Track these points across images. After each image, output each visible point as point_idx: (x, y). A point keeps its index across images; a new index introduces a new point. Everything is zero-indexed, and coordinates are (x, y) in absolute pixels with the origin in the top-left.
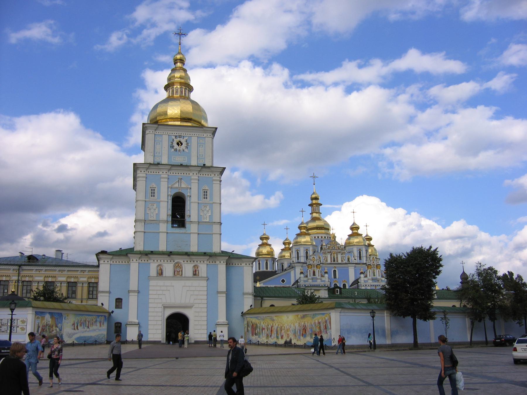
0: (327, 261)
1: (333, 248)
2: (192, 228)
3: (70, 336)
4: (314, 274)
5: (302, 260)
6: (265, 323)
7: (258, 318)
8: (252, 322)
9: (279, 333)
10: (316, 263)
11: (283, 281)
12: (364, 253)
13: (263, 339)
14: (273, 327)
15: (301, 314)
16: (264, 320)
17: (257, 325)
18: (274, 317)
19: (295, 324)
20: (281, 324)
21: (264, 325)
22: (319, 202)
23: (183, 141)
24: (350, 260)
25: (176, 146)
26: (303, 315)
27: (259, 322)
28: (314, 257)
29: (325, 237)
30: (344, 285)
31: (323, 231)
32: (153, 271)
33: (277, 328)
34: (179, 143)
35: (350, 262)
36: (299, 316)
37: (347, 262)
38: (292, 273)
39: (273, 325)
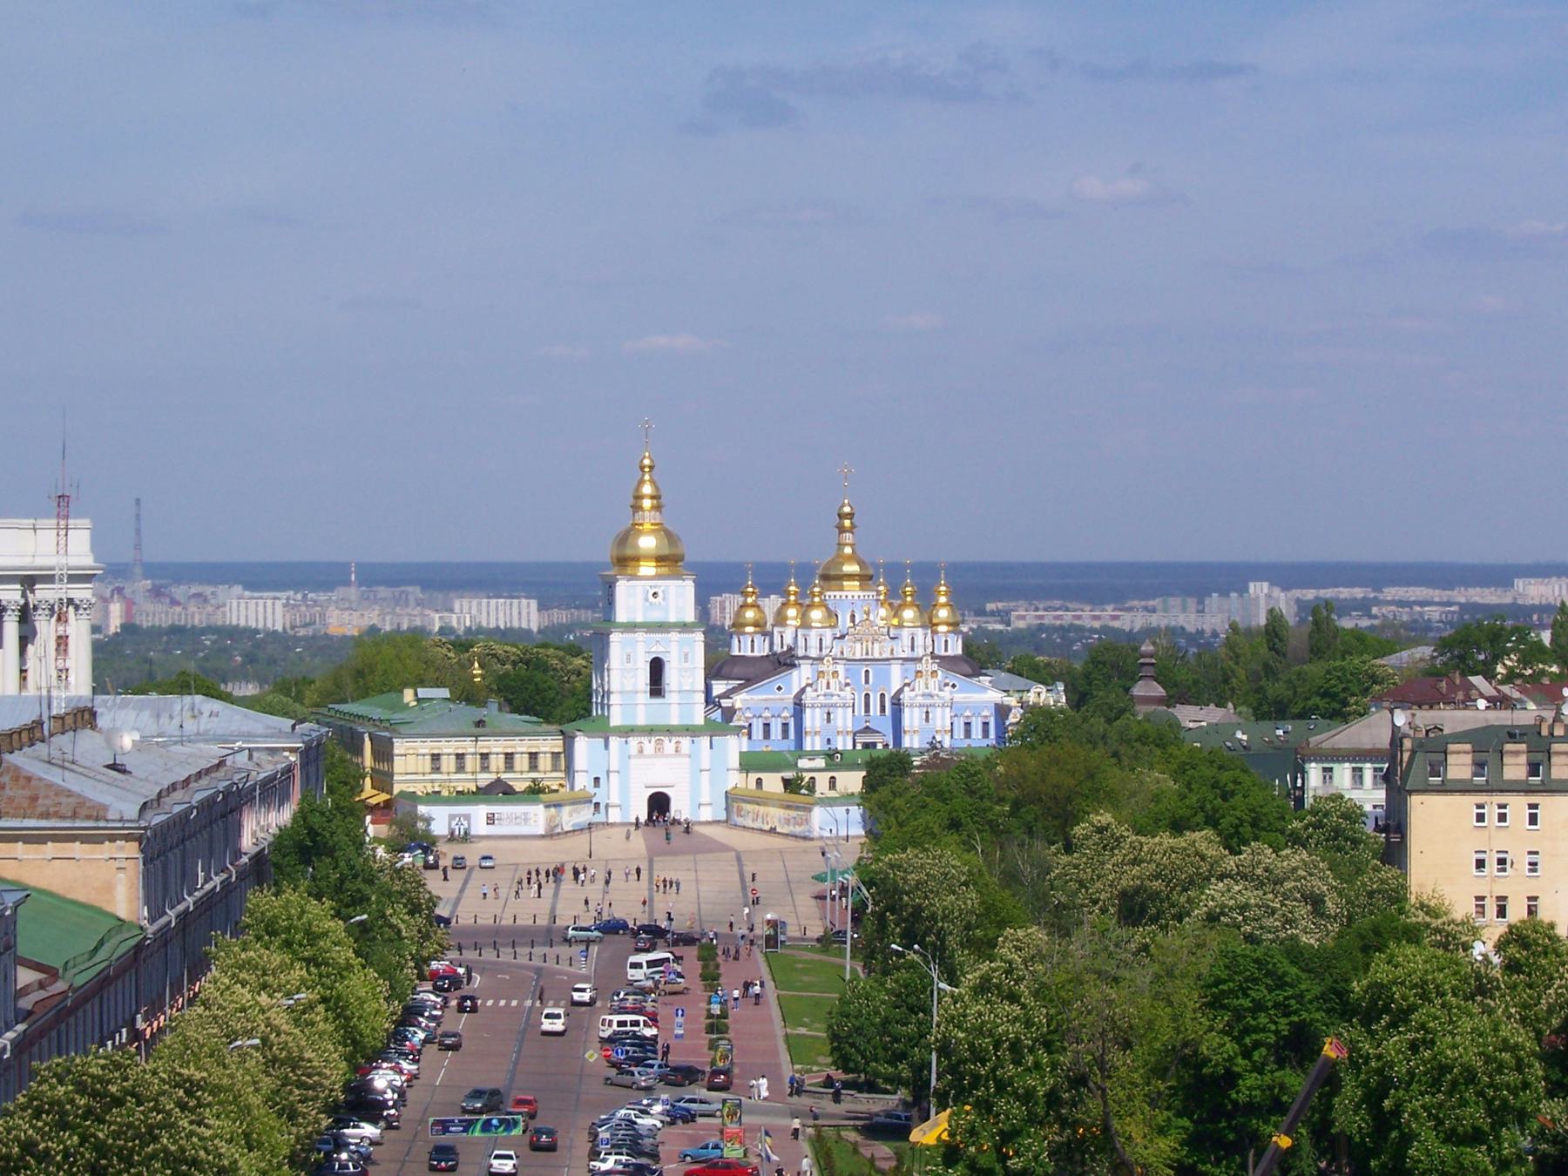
0: (854, 654)
2: (671, 697)
4: (828, 687)
5: (814, 653)
9: (764, 819)
10: (832, 669)
11: (779, 688)
12: (919, 641)
13: (749, 823)
24: (895, 652)
30: (882, 696)
34: (655, 594)
37: (889, 656)
38: (795, 673)
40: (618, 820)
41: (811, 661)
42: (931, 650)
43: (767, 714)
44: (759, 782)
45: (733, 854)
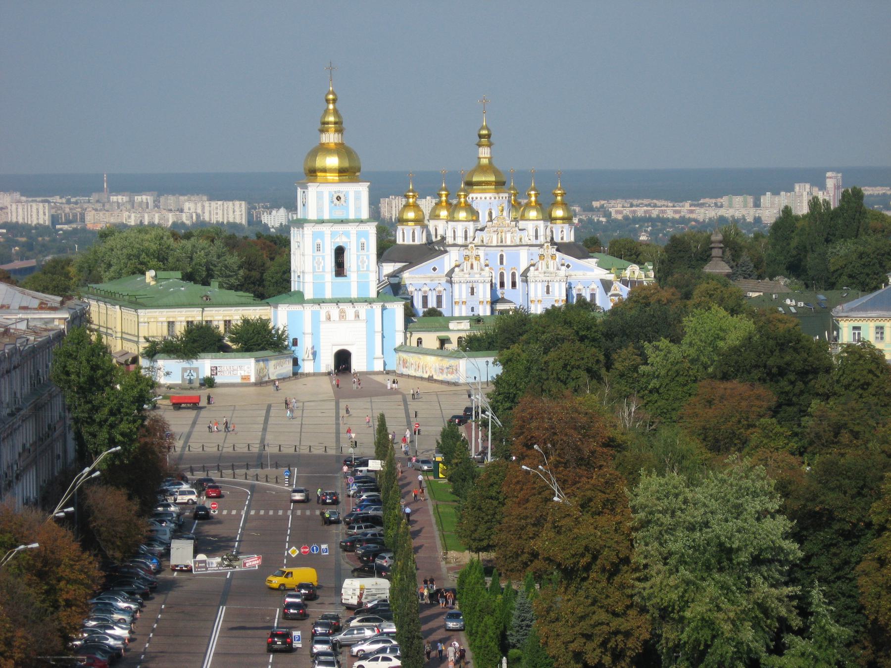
3: (273, 374)
4: (472, 267)
5: (460, 241)
10: (475, 252)
11: (434, 269)
12: (541, 232)
13: (412, 372)
15: (440, 358)
23: (341, 196)
24: (523, 240)
25: (336, 201)
29: (495, 198)
30: (513, 275)
32: (323, 317)
34: (339, 198)
35: (524, 243)
37: (518, 243)
38: (446, 257)
40: (311, 371)
41: (458, 248)
42: (549, 239)
43: (426, 288)
44: (420, 341)
45: (400, 397)
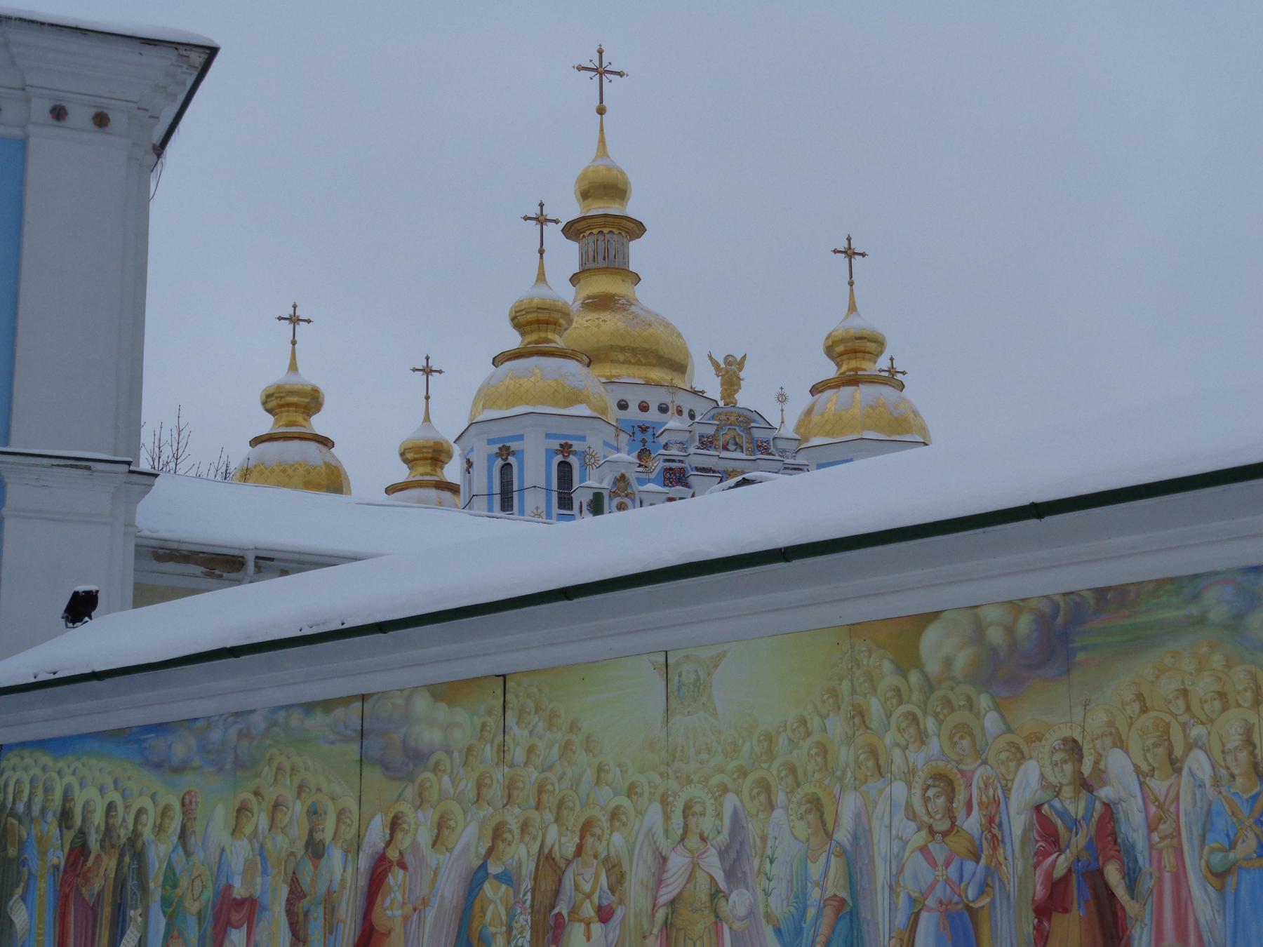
1: (731, 447)
6: (262, 819)
7: (159, 744)
8: (65, 816)
14: (395, 878)
16: (244, 765)
17: (140, 857)
18: (422, 704)
19: (849, 805)
20: (549, 816)
21: (240, 853)
22: (633, 208)
26: (1044, 621)
27: (166, 812)
28: (623, 477)
31: (657, 374)
33: (475, 881)
36: (931, 635)
39: (403, 841)
